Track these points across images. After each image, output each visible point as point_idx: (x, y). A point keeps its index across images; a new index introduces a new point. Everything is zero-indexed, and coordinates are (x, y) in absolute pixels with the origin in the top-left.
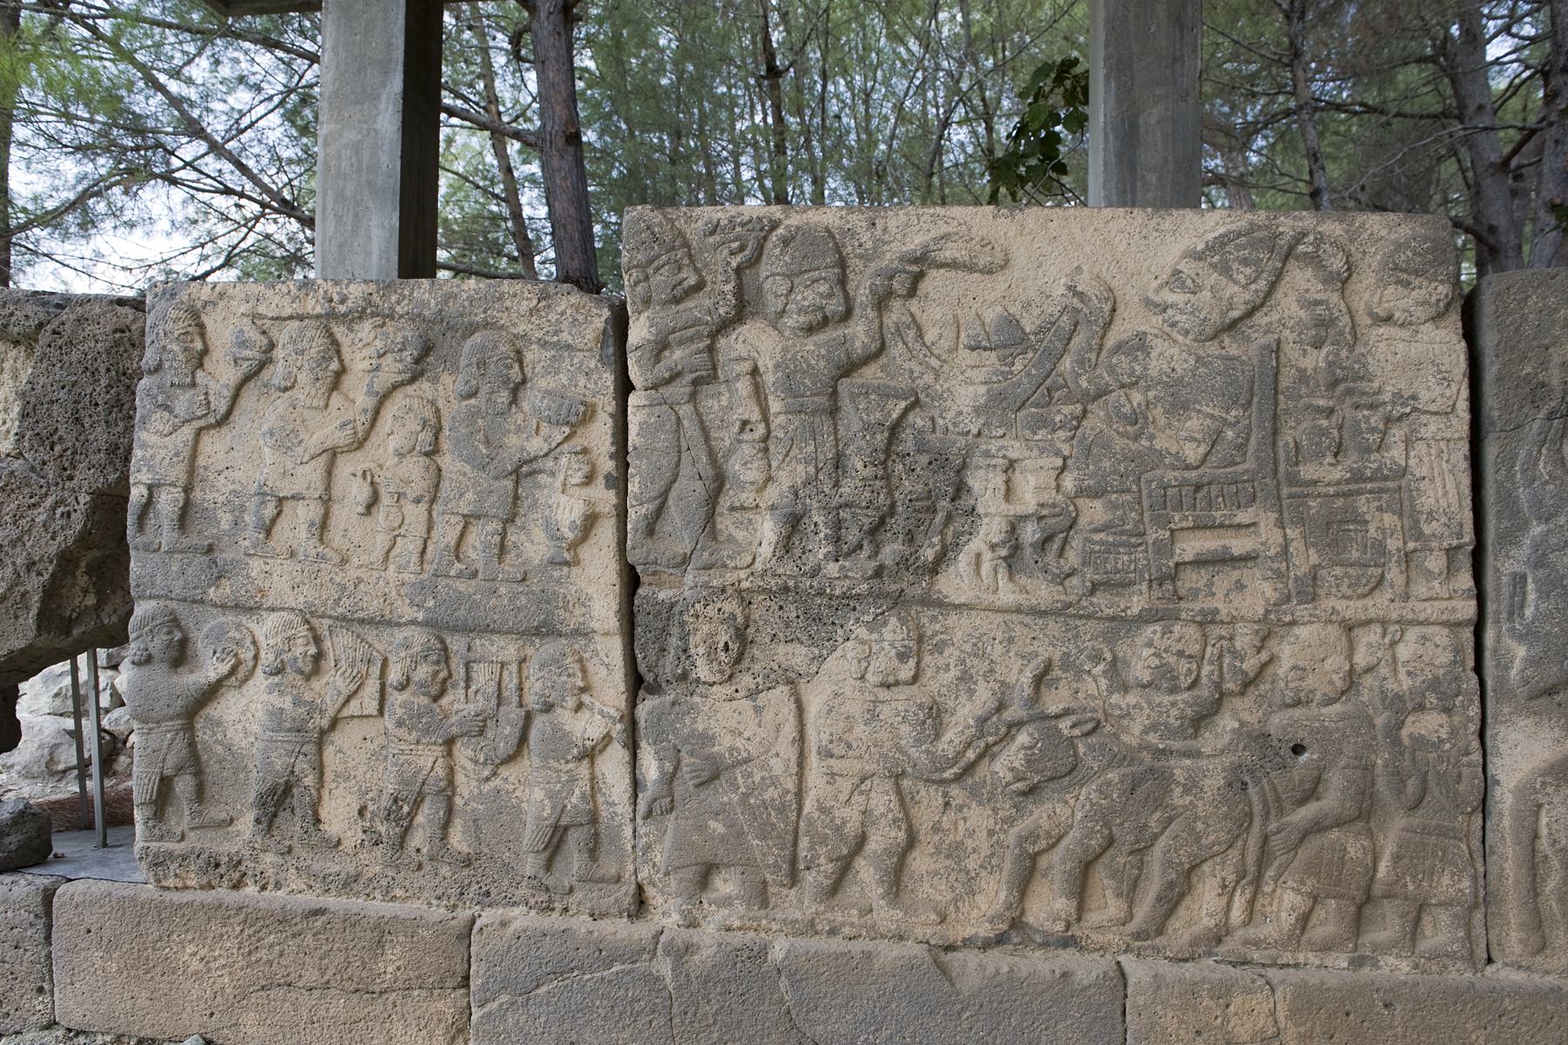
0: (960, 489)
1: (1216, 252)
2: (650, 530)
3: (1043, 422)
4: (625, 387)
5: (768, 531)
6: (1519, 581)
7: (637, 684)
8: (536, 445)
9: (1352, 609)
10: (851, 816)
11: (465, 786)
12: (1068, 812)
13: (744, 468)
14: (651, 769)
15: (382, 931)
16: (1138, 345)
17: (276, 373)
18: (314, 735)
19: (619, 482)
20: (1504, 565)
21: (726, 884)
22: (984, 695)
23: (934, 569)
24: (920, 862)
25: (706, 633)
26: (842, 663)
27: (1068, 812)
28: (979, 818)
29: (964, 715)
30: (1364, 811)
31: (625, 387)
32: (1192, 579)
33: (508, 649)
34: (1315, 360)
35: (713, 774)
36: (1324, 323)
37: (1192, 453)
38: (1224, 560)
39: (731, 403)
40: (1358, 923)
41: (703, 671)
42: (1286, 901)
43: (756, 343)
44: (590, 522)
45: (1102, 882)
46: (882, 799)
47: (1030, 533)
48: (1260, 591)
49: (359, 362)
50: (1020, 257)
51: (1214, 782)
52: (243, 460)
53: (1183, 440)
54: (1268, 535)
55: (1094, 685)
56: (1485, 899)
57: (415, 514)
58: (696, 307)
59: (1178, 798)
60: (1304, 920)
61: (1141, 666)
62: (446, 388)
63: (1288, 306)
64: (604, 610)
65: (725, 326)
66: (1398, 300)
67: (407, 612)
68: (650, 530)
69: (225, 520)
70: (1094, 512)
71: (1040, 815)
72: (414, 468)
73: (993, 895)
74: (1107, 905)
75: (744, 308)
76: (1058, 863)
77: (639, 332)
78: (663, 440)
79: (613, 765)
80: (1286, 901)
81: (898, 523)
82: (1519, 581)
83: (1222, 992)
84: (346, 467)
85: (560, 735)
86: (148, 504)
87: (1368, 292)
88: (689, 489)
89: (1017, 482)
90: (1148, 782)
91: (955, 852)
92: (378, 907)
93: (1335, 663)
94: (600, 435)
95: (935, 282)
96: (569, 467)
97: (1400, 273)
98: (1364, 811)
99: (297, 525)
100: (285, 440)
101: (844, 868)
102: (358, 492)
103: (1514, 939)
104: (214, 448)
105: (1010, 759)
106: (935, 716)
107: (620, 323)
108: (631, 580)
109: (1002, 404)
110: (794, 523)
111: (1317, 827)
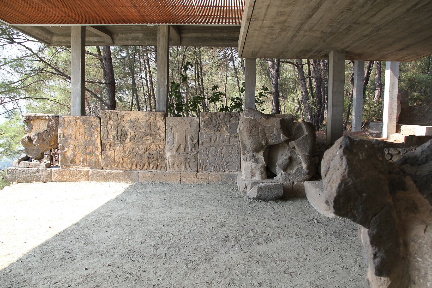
0: (127, 134)
1: (146, 115)
2: (103, 138)
3: (133, 129)
4: (101, 125)
5: (112, 138)
6: (168, 141)
7: (102, 150)
8: (93, 130)
9: (156, 144)
10: (118, 160)
11: (88, 159)
12: (136, 159)
13: (110, 133)
14: (103, 157)
15: (81, 171)
16: (140, 123)
17: (71, 124)
18: (75, 155)
19: (100, 133)
20: (167, 140)
21: (109, 166)
22: (129, 150)
23: (125, 141)
24: (124, 164)
25: (107, 145)
26: (118, 148)
27: (136, 159)
28: (129, 160)
29: (127, 152)
30: (157, 159)
31: (101, 125)
32: (144, 141)
33: (91, 147)
34: (153, 124)
35: (108, 157)
36: (154, 121)
37: (144, 131)
38: (146, 140)
39: (109, 127)
40: (157, 168)
41: (107, 149)
42: (151, 167)
43: (111, 122)
44: (98, 137)
45: (138, 165)
46: (121, 159)
47: (132, 138)
48: (150, 142)
49: (78, 123)
50: (131, 115)
51: (146, 157)
52: (68, 131)
53: (143, 130)
54: (150, 138)
55: (137, 149)
56: (166, 166)
57: (83, 136)
58: (106, 119)
59: (143, 158)
60: (153, 168)
61: (140, 149)
62: (86, 125)
63: (151, 120)
64: (99, 144)
65: (108, 121)
66: (160, 119)
67: (83, 144)
68: (103, 138)
69: (67, 137)
70: (137, 136)
71: (133, 160)
72: (83, 132)
73: (130, 166)
74: (138, 167)
75: (110, 119)
76: (134, 164)
77: (101, 121)
78: (104, 130)
79: (100, 157)
80: (151, 167)
81: (122, 137)
82: (168, 141)
83: (145, 173)
84: (77, 132)
85: (96, 154)
86: (60, 135)
87: (157, 118)
88: (106, 134)
89: (131, 133)
90: (141, 157)
91: (127, 163)
92: (80, 169)
93: (155, 148)
94: (99, 129)
95: (125, 117)
96: (96, 132)
97: (160, 117)
98: (157, 159)
99: (73, 137)
100: (72, 130)
101: (118, 165)
102: (79, 134)
103: (168, 169)
104: (66, 130)
105: (131, 156)
106: (125, 152)
107: (100, 120)
108: (101, 142)
109: (130, 127)
110: (114, 137)
111: (154, 161)
